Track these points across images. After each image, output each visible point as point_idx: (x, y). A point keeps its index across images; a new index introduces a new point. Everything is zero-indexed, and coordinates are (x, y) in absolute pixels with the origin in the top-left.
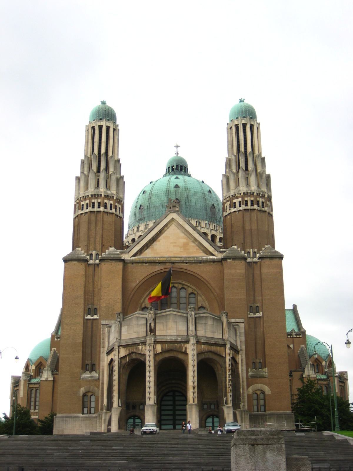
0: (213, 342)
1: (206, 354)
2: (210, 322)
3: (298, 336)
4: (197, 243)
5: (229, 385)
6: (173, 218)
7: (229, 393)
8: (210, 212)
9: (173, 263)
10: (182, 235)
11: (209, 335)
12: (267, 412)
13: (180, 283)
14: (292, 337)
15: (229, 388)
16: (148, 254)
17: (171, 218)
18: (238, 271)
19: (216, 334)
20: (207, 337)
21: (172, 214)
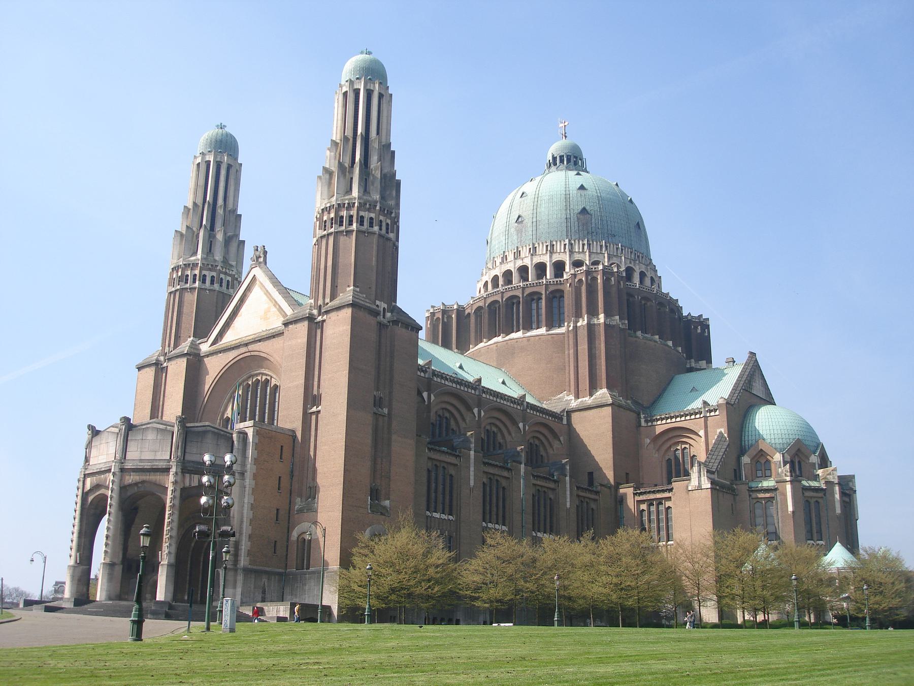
0: (147, 465)
1: (140, 485)
2: (151, 436)
3: (713, 414)
4: (278, 307)
5: (167, 530)
6: (255, 275)
7: (166, 542)
8: (576, 223)
9: (246, 345)
10: (265, 297)
11: (148, 456)
12: (311, 569)
13: (263, 374)
14: (702, 416)
15: (166, 535)
16: (230, 337)
17: (253, 275)
18: (299, 341)
19: (160, 453)
20: (141, 460)
21: (254, 269)
